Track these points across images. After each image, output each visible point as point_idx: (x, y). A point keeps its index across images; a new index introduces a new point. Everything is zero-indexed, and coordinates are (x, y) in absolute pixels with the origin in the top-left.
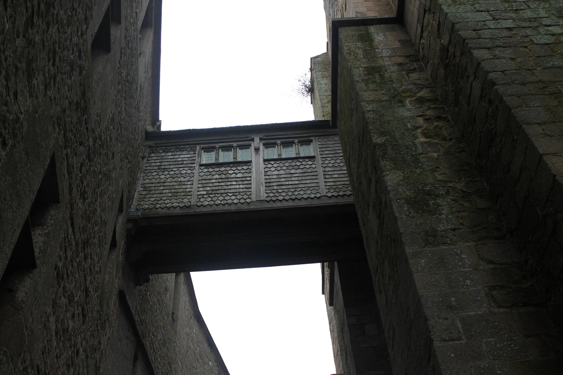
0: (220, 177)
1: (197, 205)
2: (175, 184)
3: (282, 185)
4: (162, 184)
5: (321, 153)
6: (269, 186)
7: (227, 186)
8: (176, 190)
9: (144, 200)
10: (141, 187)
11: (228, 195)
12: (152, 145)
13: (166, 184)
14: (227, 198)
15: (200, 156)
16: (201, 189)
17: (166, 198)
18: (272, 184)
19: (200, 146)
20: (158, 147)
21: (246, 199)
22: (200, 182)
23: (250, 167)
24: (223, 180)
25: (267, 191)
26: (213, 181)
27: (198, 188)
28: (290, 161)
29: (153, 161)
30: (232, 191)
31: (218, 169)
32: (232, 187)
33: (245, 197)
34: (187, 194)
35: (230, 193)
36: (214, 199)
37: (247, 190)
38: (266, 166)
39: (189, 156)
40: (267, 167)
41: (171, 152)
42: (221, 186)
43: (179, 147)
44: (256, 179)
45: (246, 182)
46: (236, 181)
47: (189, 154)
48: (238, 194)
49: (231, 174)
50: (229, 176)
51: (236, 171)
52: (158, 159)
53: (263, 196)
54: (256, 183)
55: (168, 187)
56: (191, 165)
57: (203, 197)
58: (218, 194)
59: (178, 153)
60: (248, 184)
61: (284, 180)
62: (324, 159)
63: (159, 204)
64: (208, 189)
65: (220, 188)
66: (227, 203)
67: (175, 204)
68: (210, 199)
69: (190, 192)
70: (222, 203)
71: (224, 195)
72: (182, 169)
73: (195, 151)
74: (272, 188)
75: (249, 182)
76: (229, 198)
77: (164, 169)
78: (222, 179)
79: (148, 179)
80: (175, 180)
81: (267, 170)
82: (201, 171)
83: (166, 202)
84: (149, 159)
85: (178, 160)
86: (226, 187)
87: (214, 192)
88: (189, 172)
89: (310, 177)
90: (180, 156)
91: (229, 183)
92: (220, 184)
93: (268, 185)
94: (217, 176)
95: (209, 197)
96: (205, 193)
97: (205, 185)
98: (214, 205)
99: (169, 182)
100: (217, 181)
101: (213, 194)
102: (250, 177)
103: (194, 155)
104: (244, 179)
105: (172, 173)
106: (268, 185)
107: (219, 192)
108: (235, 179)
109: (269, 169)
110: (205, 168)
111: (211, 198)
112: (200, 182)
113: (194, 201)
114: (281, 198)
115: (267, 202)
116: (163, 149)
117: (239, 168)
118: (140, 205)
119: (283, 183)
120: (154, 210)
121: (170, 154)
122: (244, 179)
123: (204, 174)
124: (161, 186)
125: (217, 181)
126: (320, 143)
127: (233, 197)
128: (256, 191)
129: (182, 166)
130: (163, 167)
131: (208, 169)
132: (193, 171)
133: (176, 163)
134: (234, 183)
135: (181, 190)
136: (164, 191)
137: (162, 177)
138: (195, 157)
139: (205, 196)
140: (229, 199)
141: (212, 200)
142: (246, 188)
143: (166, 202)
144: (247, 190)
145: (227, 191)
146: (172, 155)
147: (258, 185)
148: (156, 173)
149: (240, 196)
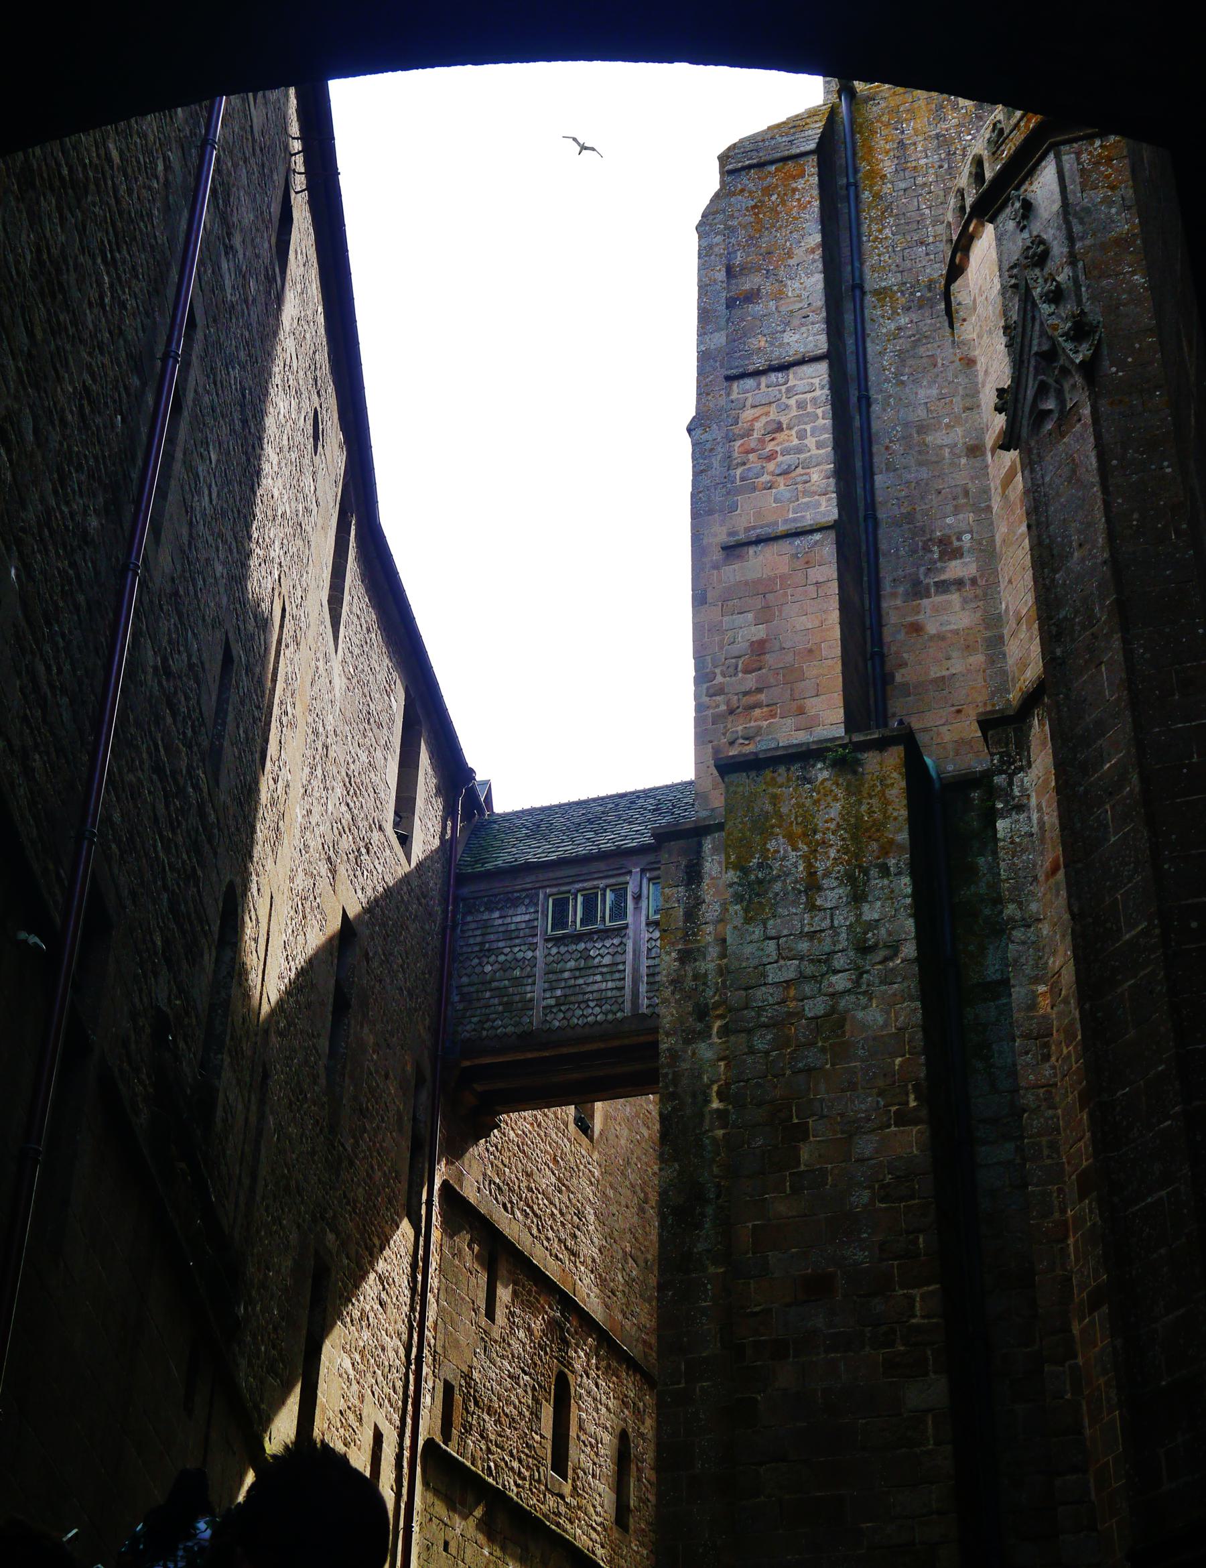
7: (588, 984)
13: (494, 984)
16: (548, 995)
20: (477, 898)
23: (624, 940)
24: (583, 973)
26: (566, 975)
31: (574, 947)
32: (595, 987)
33: (615, 1008)
34: (528, 1005)
35: (592, 1000)
38: (650, 936)
39: (527, 917)
45: (617, 976)
46: (602, 973)
49: (594, 958)
50: (590, 963)
59: (510, 913)
64: (559, 993)
67: (510, 1029)
71: (583, 1006)
73: (536, 904)
76: (590, 1011)
77: (489, 950)
80: (508, 974)
88: (529, 954)
91: (591, 980)
94: (572, 964)
95: (560, 1010)
96: (552, 1002)
105: (502, 958)
106: (652, 980)
111: (564, 1013)
121: (497, 914)
127: (597, 1010)
129: (517, 941)
134: (599, 978)
137: (488, 968)
139: (554, 1010)
148: (476, 961)
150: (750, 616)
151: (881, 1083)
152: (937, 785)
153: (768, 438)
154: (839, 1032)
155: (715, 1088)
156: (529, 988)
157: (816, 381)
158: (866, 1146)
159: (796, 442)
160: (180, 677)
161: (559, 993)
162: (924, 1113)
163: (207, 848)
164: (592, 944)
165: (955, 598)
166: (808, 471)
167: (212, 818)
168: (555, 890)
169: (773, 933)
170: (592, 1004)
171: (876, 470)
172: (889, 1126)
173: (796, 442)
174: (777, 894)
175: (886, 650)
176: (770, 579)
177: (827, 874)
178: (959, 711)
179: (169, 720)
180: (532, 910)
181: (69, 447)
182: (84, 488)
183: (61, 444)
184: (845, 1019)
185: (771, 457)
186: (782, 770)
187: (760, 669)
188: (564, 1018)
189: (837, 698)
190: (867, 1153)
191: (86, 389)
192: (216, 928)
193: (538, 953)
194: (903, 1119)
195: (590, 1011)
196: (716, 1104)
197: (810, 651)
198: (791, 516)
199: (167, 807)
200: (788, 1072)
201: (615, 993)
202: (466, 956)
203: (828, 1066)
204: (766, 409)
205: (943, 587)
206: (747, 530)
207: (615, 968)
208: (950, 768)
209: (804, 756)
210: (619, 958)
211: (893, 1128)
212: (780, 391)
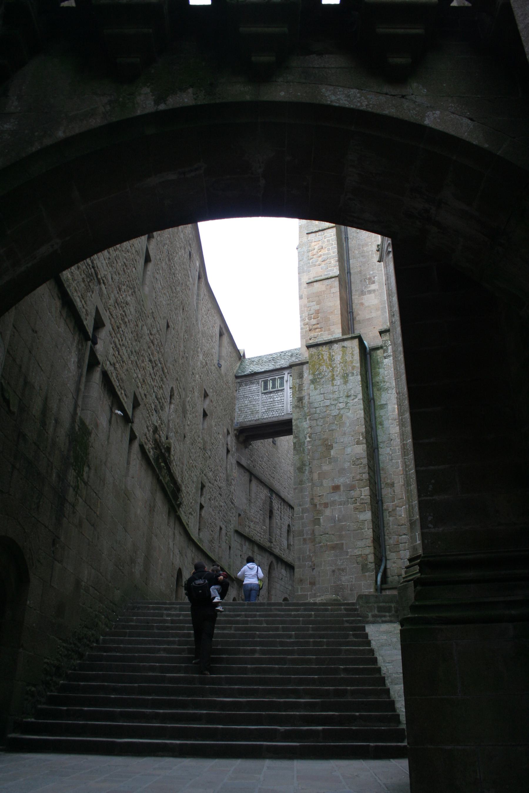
7: (274, 406)
13: (248, 406)
14: (274, 413)
16: (263, 409)
20: (242, 382)
23: (283, 393)
26: (268, 403)
30: (276, 409)
32: (276, 406)
39: (256, 387)
45: (282, 403)
46: (278, 402)
60: (283, 404)
64: (266, 408)
65: (271, 407)
67: (253, 418)
69: (258, 411)
70: (272, 416)
71: (273, 411)
72: (254, 396)
73: (259, 384)
80: (251, 403)
87: (268, 410)
88: (257, 398)
91: (274, 404)
94: (269, 400)
96: (264, 411)
103: (258, 387)
105: (250, 399)
107: (270, 410)
110: (264, 395)
112: (262, 404)
117: (279, 394)
118: (238, 420)
121: (248, 387)
122: (281, 401)
129: (254, 394)
134: (277, 404)
136: (248, 411)
141: (268, 415)
145: (273, 409)
146: (249, 387)
150: (315, 303)
151: (352, 433)
152: (368, 349)
153: (319, 250)
154: (341, 419)
155: (308, 435)
156: (258, 407)
157: (332, 234)
158: (349, 450)
159: (327, 252)
160: (155, 335)
161: (266, 408)
162: (364, 441)
163: (165, 379)
164: (275, 394)
165: (373, 295)
166: (330, 260)
167: (166, 371)
168: (264, 379)
169: (322, 392)
170: (275, 411)
171: (350, 258)
172: (355, 445)
173: (327, 252)
174: (323, 381)
175: (354, 311)
176: (320, 292)
177: (337, 376)
178: (374, 328)
179: (153, 347)
181: (121, 280)
182: (125, 290)
183: (119, 280)
184: (342, 416)
185: (320, 256)
186: (324, 346)
187: (318, 318)
188: (268, 415)
189: (340, 326)
190: (348, 453)
191: (125, 263)
192: (169, 400)
193: (260, 397)
194: (358, 443)
196: (308, 439)
197: (332, 312)
198: (326, 273)
199: (153, 370)
200: (327, 431)
201: (282, 408)
203: (338, 429)
204: (318, 242)
205: (370, 292)
206: (314, 278)
207: (281, 402)
208: (372, 344)
209: (330, 343)
210: (283, 398)
211: (356, 446)
212: (322, 237)
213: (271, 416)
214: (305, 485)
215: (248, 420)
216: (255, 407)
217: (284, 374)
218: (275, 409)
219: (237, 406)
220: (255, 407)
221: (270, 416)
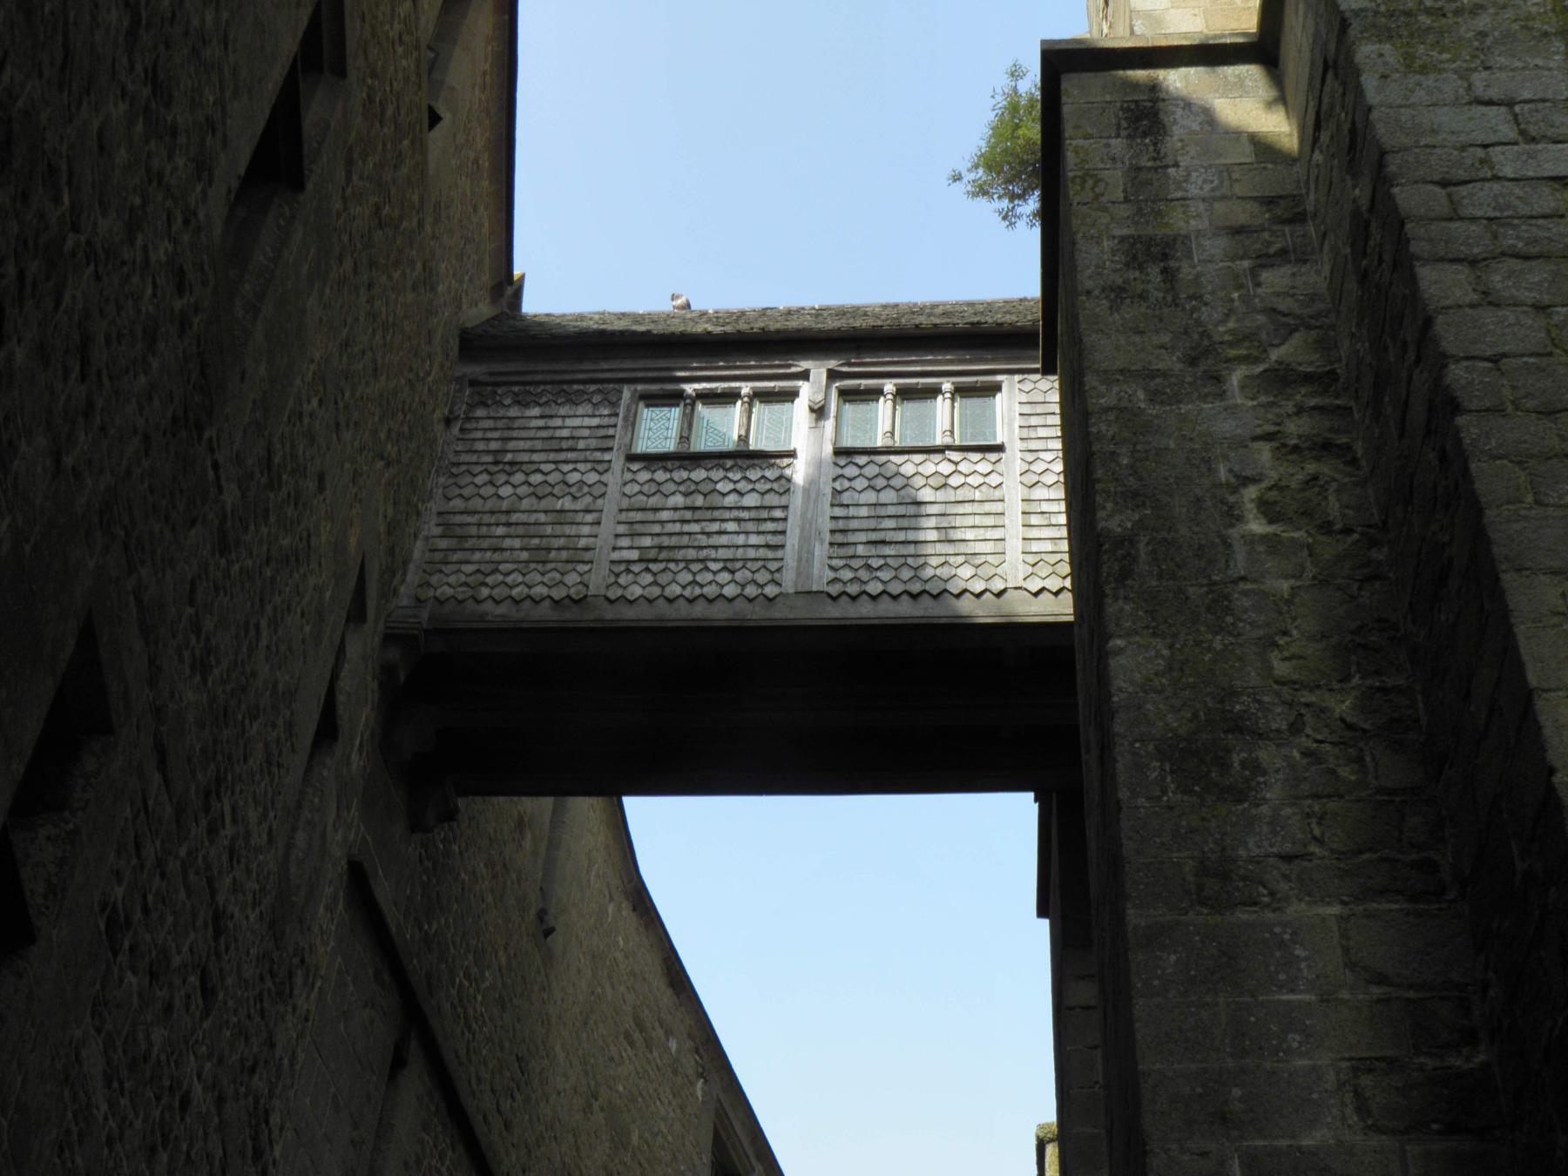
0: (689, 502)
1: (607, 599)
2: (542, 517)
3: (883, 542)
4: (503, 518)
5: (1025, 433)
6: (841, 545)
7: (709, 534)
8: (544, 540)
9: (443, 569)
10: (438, 525)
11: (707, 569)
12: (481, 378)
13: (514, 518)
15: (632, 422)
16: (625, 542)
17: (511, 567)
18: (851, 538)
19: (633, 387)
20: (498, 384)
21: (765, 584)
22: (623, 516)
24: (698, 515)
25: (834, 562)
26: (665, 515)
27: (617, 536)
28: (918, 458)
29: (479, 434)
30: (722, 553)
31: (685, 475)
32: (724, 540)
33: (762, 577)
34: (579, 556)
35: (715, 560)
36: (664, 579)
37: (770, 554)
38: (840, 471)
39: (595, 422)
40: (842, 476)
41: (540, 405)
42: (690, 534)
43: (565, 387)
44: (803, 515)
45: (770, 526)
46: (738, 520)
47: (594, 416)
48: (739, 565)
49: (724, 495)
50: (716, 500)
51: (742, 486)
52: (496, 429)
53: (820, 577)
54: (802, 529)
55: (521, 530)
56: (598, 455)
57: (628, 571)
58: (676, 561)
59: (563, 411)
60: (774, 533)
61: (891, 523)
62: (1030, 457)
63: (486, 585)
64: (647, 542)
65: (685, 540)
66: (702, 595)
67: (540, 590)
68: (648, 578)
69: (587, 549)
70: (687, 593)
71: (695, 567)
72: (571, 467)
73: (614, 404)
74: (850, 551)
75: (779, 526)
77: (511, 463)
78: (694, 509)
79: (461, 496)
80: (544, 504)
81: (841, 484)
82: (628, 476)
83: (509, 579)
84: (468, 426)
85: (558, 433)
86: (703, 540)
87: (664, 555)
88: (592, 478)
89: (978, 520)
90: (569, 422)
91: (715, 527)
92: (687, 528)
93: (839, 538)
94: (678, 500)
95: (647, 570)
96: (634, 555)
97: (639, 528)
98: (661, 601)
99: (523, 512)
100: (677, 516)
101: (661, 561)
102: (785, 508)
103: (612, 421)
104: (765, 514)
106: (839, 538)
107: (680, 554)
108: (735, 514)
109: (847, 484)
110: (645, 468)
111: (655, 574)
112: (623, 516)
113: (598, 580)
114: (874, 588)
115: (829, 600)
116: (516, 394)
117: (754, 474)
118: (428, 584)
119: (889, 536)
120: (470, 605)
121: (536, 411)
122: (765, 514)
123: (637, 488)
124: (497, 525)
125: (677, 516)
126: (1024, 398)
127: (724, 577)
128: (800, 560)
129: (571, 456)
130: (509, 457)
131: (654, 472)
132: (604, 478)
133: (555, 446)
134: (731, 526)
135: (562, 542)
136: (508, 543)
137: (506, 491)
138: (615, 426)
139: (636, 568)
140: (710, 583)
141: (655, 583)
142: (768, 546)
143: (509, 579)
144: (770, 554)
146: (542, 417)
147: (805, 539)
148: (485, 477)
149: (747, 572)
156: (586, 530)
170: (714, 566)
180: (606, 412)
188: (655, 583)
195: (709, 577)
202: (463, 468)
210: (771, 499)
213: (677, 590)
214: (1269, 916)
215: (499, 592)
216: (569, 530)
217: (805, 376)
218: (713, 554)
219: (435, 506)
220: (569, 530)
221: (675, 590)
